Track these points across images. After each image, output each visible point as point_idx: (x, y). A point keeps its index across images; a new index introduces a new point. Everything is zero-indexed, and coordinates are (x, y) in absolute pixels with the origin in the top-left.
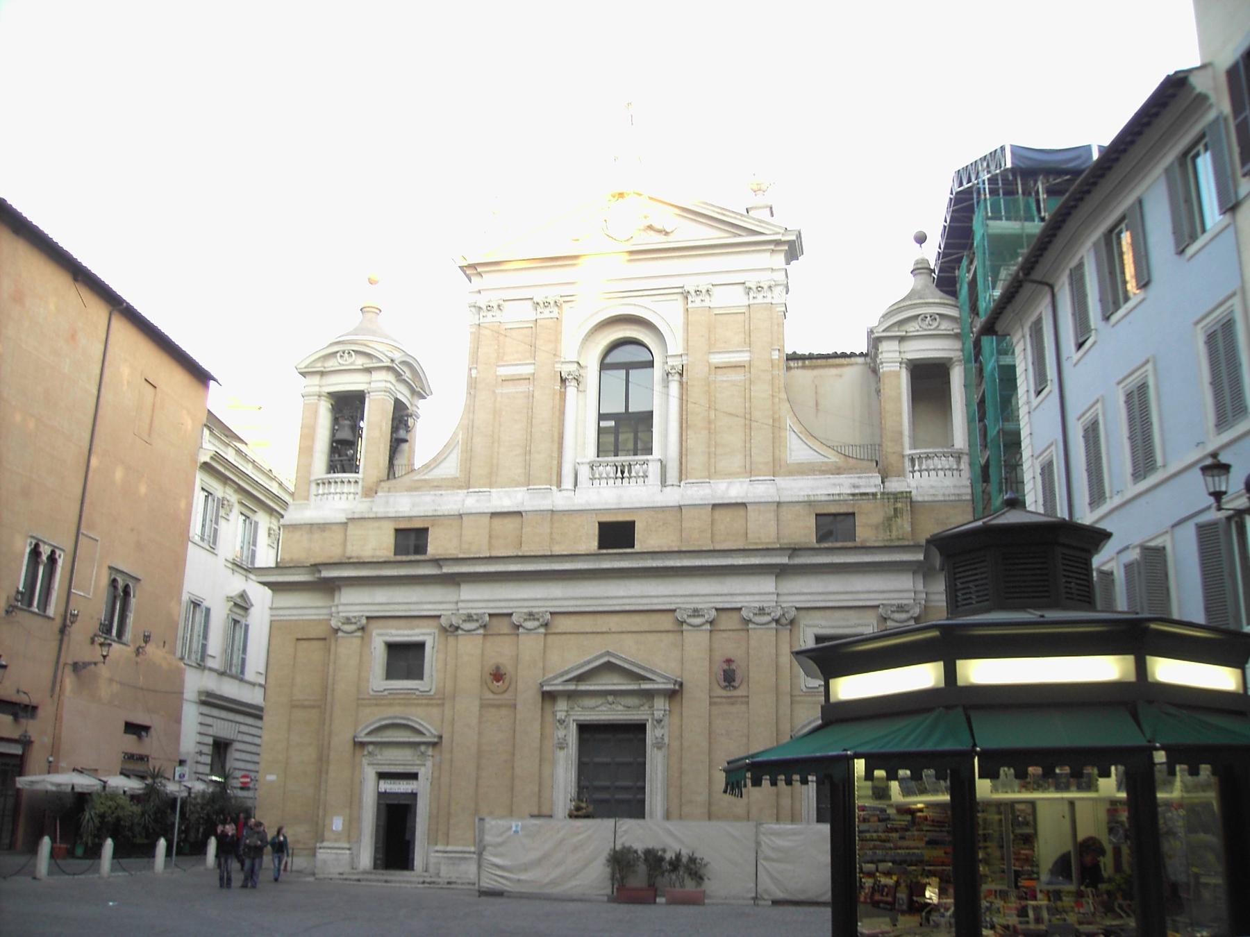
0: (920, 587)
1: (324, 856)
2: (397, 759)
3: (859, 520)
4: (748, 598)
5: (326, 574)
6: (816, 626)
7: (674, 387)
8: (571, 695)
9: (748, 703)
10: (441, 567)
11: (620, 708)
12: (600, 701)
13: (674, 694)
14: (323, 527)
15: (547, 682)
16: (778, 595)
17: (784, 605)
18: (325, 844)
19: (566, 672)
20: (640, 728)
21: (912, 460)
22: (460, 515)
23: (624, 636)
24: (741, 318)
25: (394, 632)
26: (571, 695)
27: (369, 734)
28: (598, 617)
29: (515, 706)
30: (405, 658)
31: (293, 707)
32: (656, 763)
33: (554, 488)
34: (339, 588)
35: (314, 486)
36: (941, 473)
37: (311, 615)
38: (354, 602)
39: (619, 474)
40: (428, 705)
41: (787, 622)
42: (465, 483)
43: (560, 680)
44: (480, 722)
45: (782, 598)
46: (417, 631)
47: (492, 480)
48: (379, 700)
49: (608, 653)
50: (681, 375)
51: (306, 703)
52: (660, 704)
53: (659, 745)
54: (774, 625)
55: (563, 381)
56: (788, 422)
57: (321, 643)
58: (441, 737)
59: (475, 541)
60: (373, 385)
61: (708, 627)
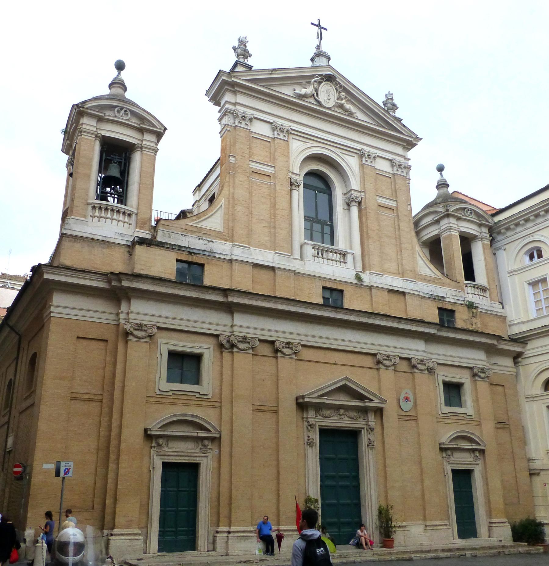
1: (118, 543)
5: (125, 283)
7: (355, 210)
10: (227, 296)
11: (346, 418)
14: (105, 243)
18: (116, 531)
22: (231, 261)
23: (343, 367)
24: (389, 180)
25: (176, 342)
26: (318, 408)
28: (327, 352)
29: (276, 412)
30: (185, 364)
31: (72, 399)
34: (129, 300)
35: (90, 208)
37: (94, 317)
38: (141, 311)
40: (207, 406)
42: (228, 236)
46: (196, 345)
47: (249, 241)
48: (163, 398)
49: (346, 379)
50: (360, 203)
51: (86, 396)
52: (371, 417)
53: (371, 445)
54: (426, 372)
57: (102, 344)
59: (243, 281)
60: (144, 142)
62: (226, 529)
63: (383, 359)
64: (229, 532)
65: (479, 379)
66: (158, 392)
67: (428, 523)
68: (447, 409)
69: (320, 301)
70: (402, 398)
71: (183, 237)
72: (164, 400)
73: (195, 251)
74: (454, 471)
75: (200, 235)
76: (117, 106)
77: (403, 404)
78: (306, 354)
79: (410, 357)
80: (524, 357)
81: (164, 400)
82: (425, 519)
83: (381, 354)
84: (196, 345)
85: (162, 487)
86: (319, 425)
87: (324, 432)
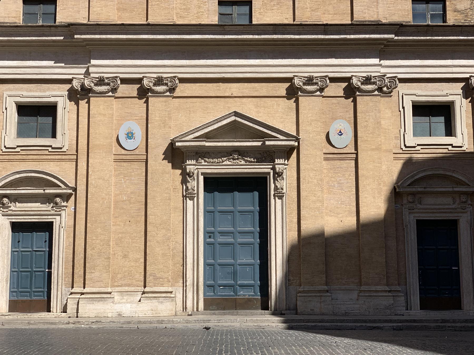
2: (33, 211)
15: (180, 138)
19: (197, 130)
23: (244, 99)
26: (200, 154)
43: (192, 136)
49: (236, 114)
62: (81, 290)
64: (82, 294)
66: (4, 150)
67: (363, 288)
69: (214, 20)
72: (12, 157)
74: (419, 222)
78: (182, 89)
79: (349, 75)
81: (12, 157)
82: (360, 284)
83: (300, 77)
84: (47, 93)
85: (418, 245)
86: (202, 174)
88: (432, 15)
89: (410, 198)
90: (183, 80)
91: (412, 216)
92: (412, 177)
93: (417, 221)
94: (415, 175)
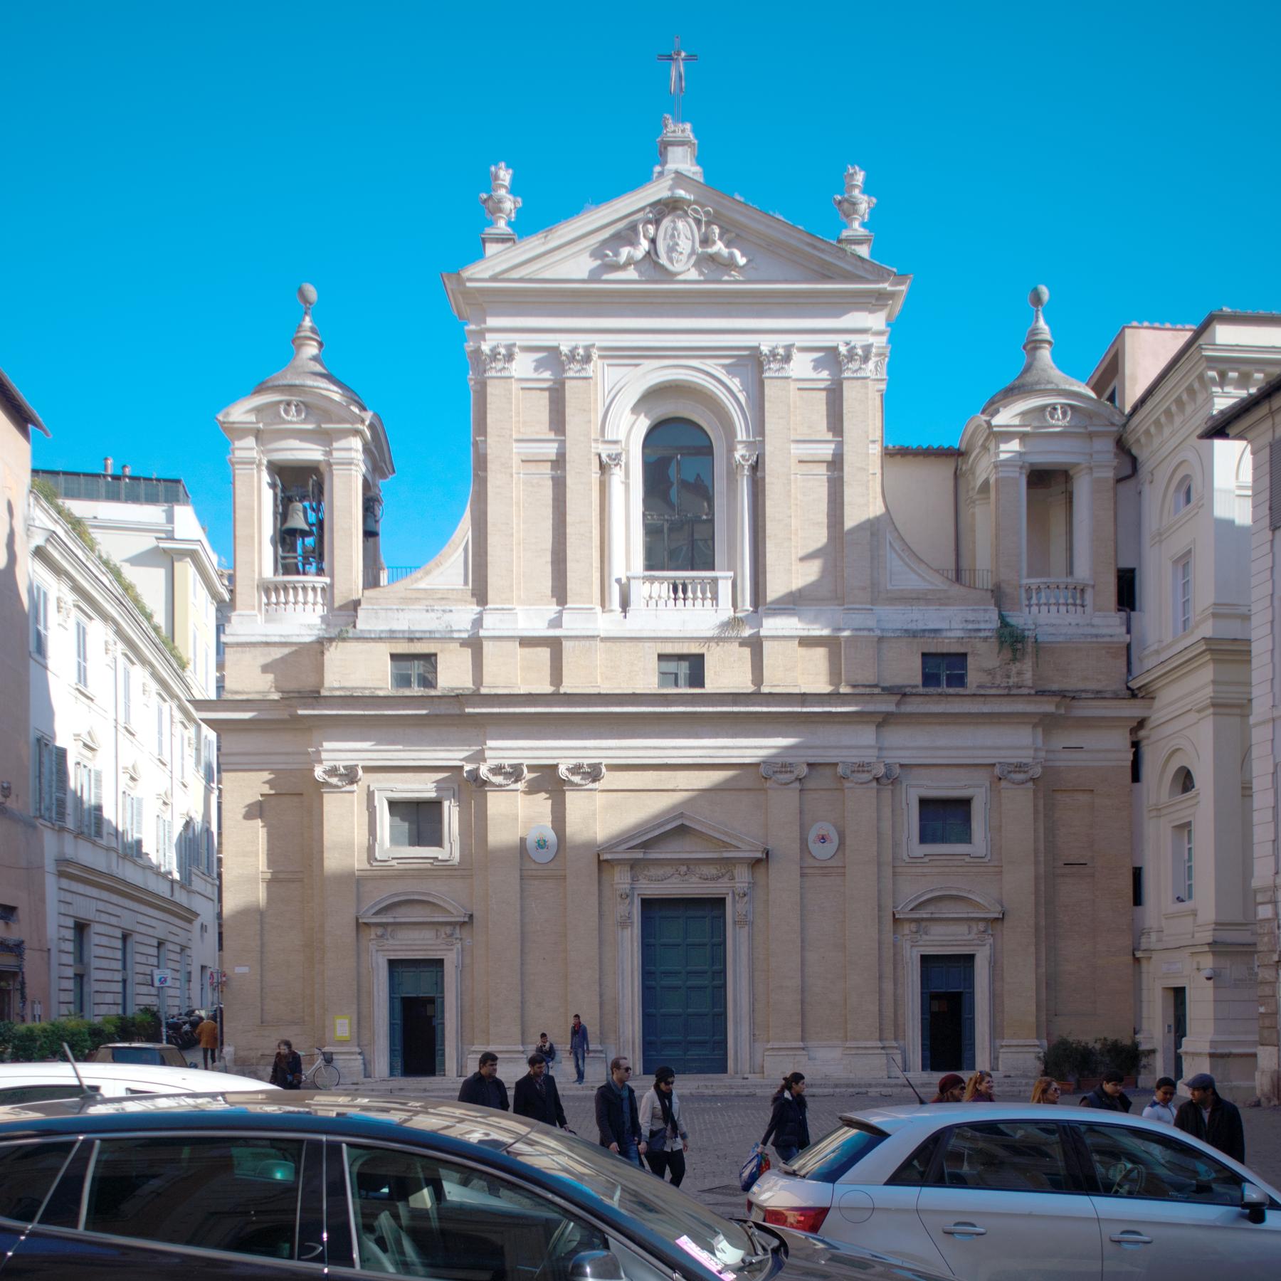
0: (1040, 743)
3: (970, 659)
4: (845, 752)
6: (921, 786)
8: (634, 865)
9: (844, 874)
12: (669, 870)
13: (760, 863)
16: (880, 749)
17: (887, 761)
20: (720, 902)
21: (1029, 590)
27: (377, 913)
29: (564, 878)
32: (737, 944)
33: (599, 608)
36: (1063, 609)
39: (680, 594)
41: (888, 780)
44: (521, 898)
45: (885, 753)
54: (874, 784)
55: (603, 467)
56: (888, 536)
58: (471, 916)
60: (336, 454)
61: (797, 785)
63: (775, 772)
65: (1010, 785)
67: (848, 1044)
68: (921, 850)
70: (812, 836)
71: (401, 615)
73: (418, 635)
75: (431, 602)
76: (280, 402)
77: (815, 848)
80: (1151, 726)
87: (649, 905)
88: (949, 677)
89: (913, 926)
90: (612, 768)
91: (915, 949)
92: (916, 898)
93: (922, 956)
94: (920, 896)
